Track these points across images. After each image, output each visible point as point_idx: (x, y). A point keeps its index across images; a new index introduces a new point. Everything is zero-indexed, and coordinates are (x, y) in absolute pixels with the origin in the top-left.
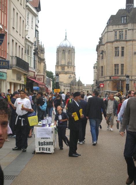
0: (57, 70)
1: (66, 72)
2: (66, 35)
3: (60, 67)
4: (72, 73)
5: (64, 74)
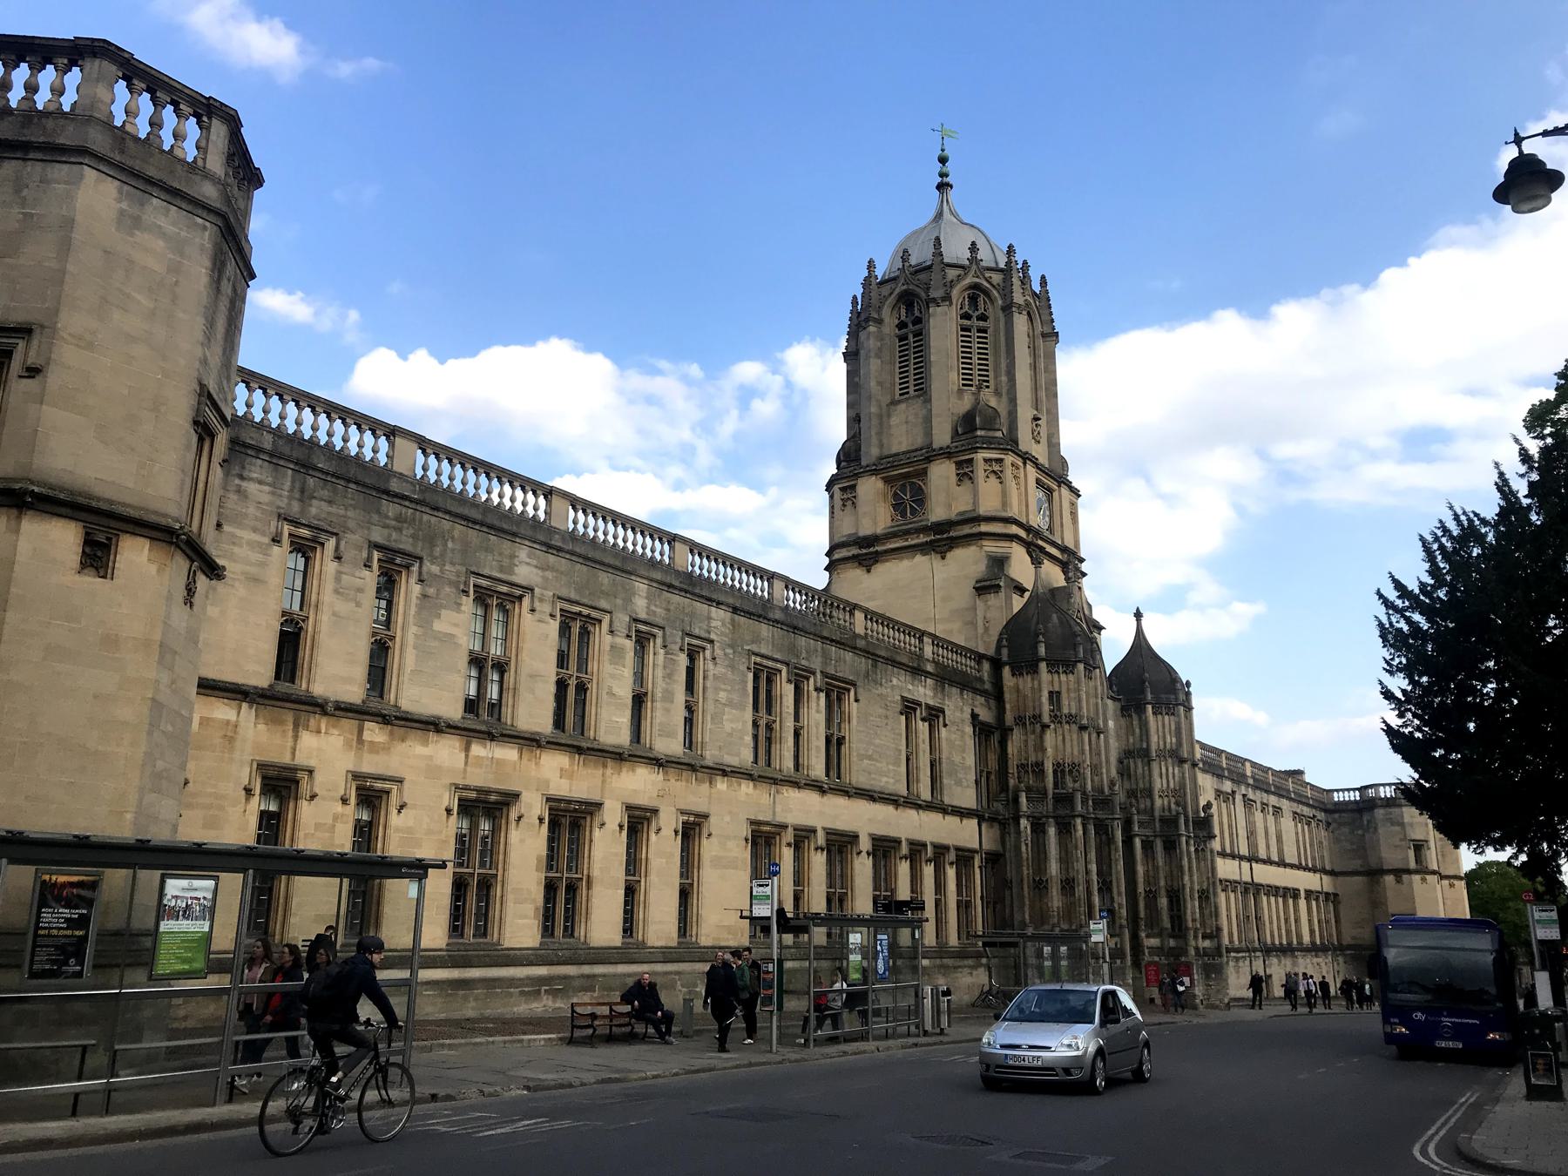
0: (847, 529)
3: (870, 488)
5: (923, 549)
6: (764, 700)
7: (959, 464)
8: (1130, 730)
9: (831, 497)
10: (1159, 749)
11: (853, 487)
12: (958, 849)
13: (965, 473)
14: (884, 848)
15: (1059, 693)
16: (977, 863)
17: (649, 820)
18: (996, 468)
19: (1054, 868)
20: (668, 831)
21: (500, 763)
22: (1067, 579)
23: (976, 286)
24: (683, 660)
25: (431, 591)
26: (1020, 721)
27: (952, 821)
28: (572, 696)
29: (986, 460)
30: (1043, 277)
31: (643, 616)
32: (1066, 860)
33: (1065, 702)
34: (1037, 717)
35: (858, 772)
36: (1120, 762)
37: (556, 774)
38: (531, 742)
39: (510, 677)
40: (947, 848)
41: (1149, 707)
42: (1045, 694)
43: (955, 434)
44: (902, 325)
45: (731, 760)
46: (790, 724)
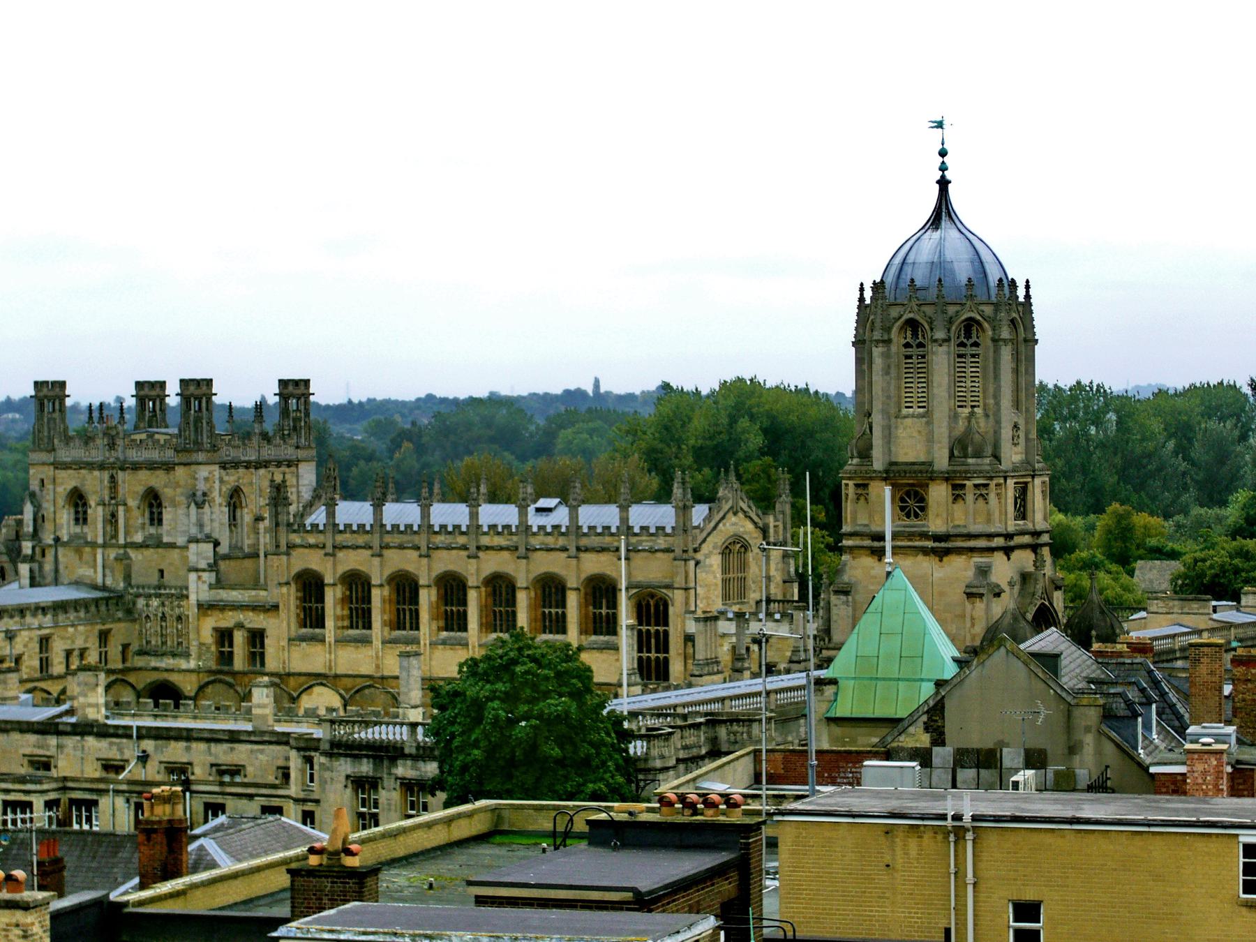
1: (937, 538)
4: (999, 542)
5: (926, 551)
7: (955, 487)
11: (865, 486)
13: (958, 493)
18: (984, 492)
23: (971, 319)
29: (976, 486)
30: (1027, 281)
43: (952, 456)
44: (907, 345)
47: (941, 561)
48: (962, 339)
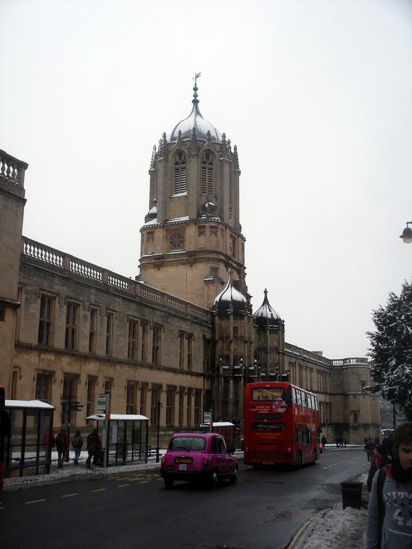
2: (195, 96)
6: (133, 333)
7: (200, 228)
8: (260, 339)
9: (142, 236)
10: (271, 348)
12: (196, 389)
13: (201, 231)
14: (171, 390)
15: (237, 328)
16: (202, 394)
17: (95, 381)
19: (231, 396)
20: (100, 385)
21: (49, 360)
22: (240, 278)
24: (106, 318)
25: (29, 297)
26: (221, 338)
27: (194, 378)
28: (71, 334)
29: (211, 227)
30: (235, 146)
31: (93, 303)
32: (236, 393)
33: (239, 331)
34: (228, 337)
35: (164, 360)
36: (255, 352)
37: (65, 365)
38: (59, 353)
39: (51, 328)
40: (192, 389)
41: (268, 331)
42: (232, 328)
44: (177, 163)
45: (121, 357)
46: (140, 343)
47: (192, 267)
48: (204, 159)
